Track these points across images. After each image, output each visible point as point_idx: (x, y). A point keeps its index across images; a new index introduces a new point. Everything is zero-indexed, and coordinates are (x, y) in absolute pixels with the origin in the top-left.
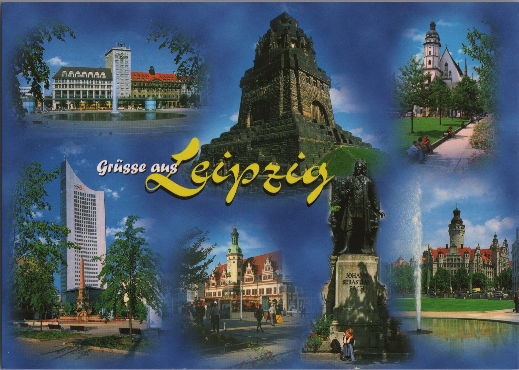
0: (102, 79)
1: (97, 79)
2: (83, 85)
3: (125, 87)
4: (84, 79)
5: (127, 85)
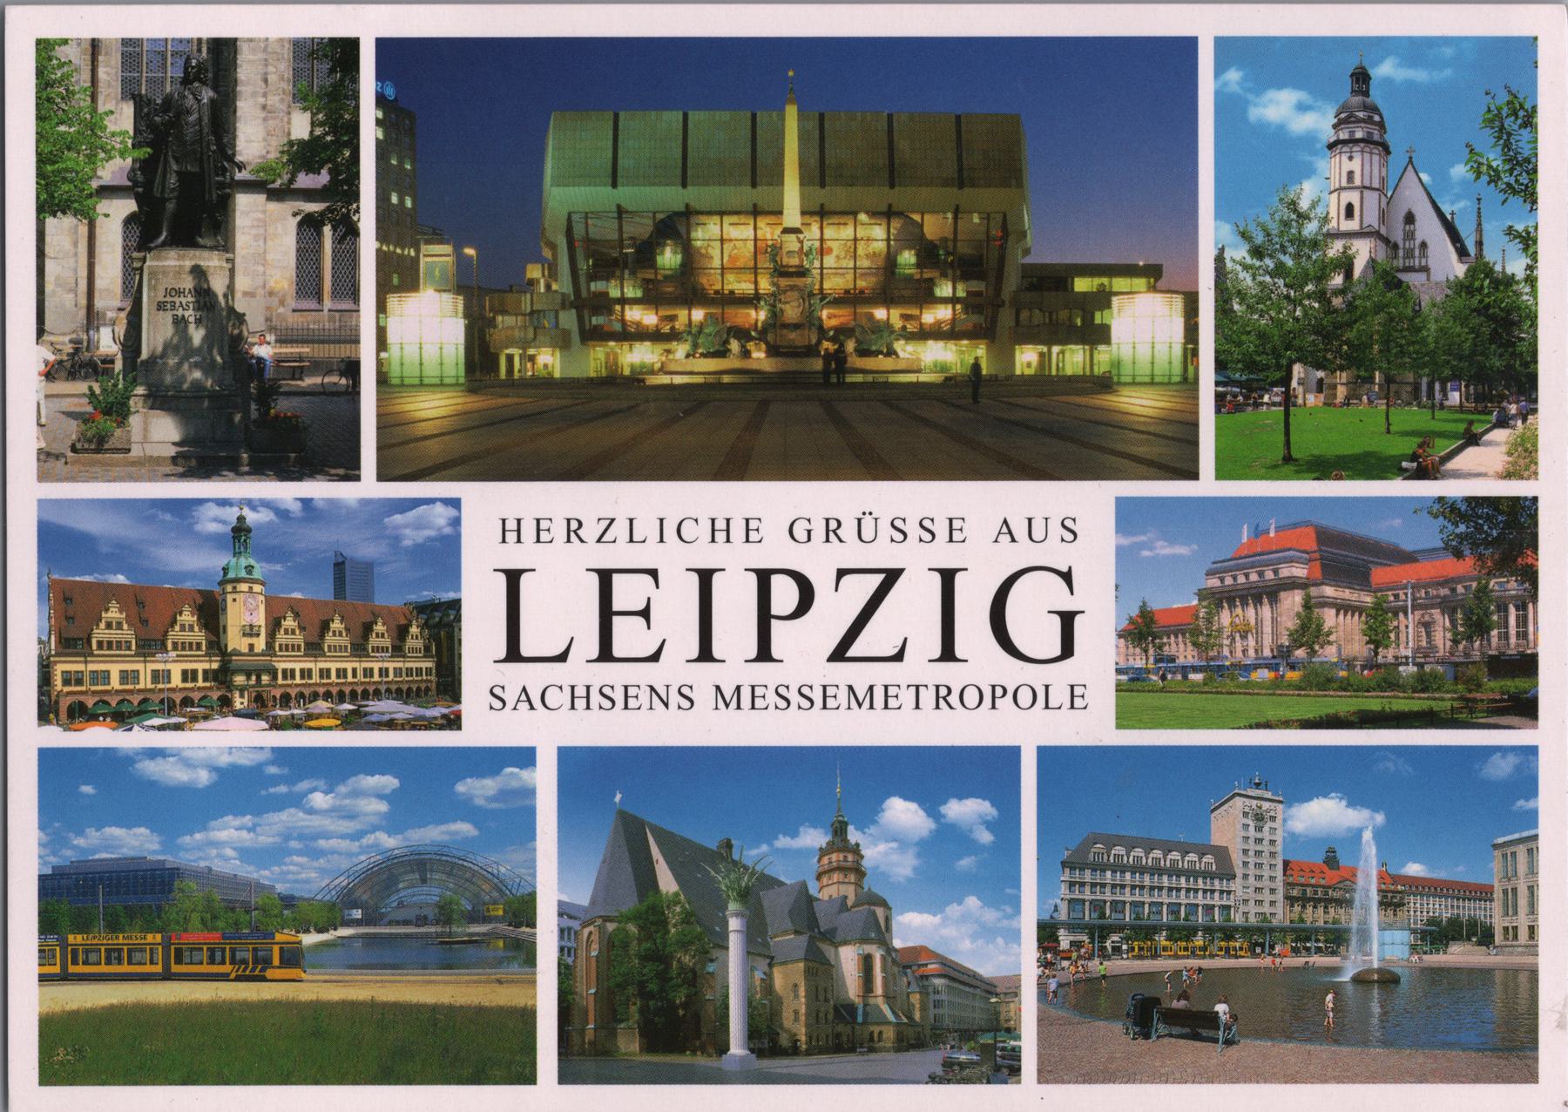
0: (1207, 875)
1: (1191, 873)
2: (1152, 888)
3: (1266, 896)
4: (1157, 870)
5: (1273, 891)
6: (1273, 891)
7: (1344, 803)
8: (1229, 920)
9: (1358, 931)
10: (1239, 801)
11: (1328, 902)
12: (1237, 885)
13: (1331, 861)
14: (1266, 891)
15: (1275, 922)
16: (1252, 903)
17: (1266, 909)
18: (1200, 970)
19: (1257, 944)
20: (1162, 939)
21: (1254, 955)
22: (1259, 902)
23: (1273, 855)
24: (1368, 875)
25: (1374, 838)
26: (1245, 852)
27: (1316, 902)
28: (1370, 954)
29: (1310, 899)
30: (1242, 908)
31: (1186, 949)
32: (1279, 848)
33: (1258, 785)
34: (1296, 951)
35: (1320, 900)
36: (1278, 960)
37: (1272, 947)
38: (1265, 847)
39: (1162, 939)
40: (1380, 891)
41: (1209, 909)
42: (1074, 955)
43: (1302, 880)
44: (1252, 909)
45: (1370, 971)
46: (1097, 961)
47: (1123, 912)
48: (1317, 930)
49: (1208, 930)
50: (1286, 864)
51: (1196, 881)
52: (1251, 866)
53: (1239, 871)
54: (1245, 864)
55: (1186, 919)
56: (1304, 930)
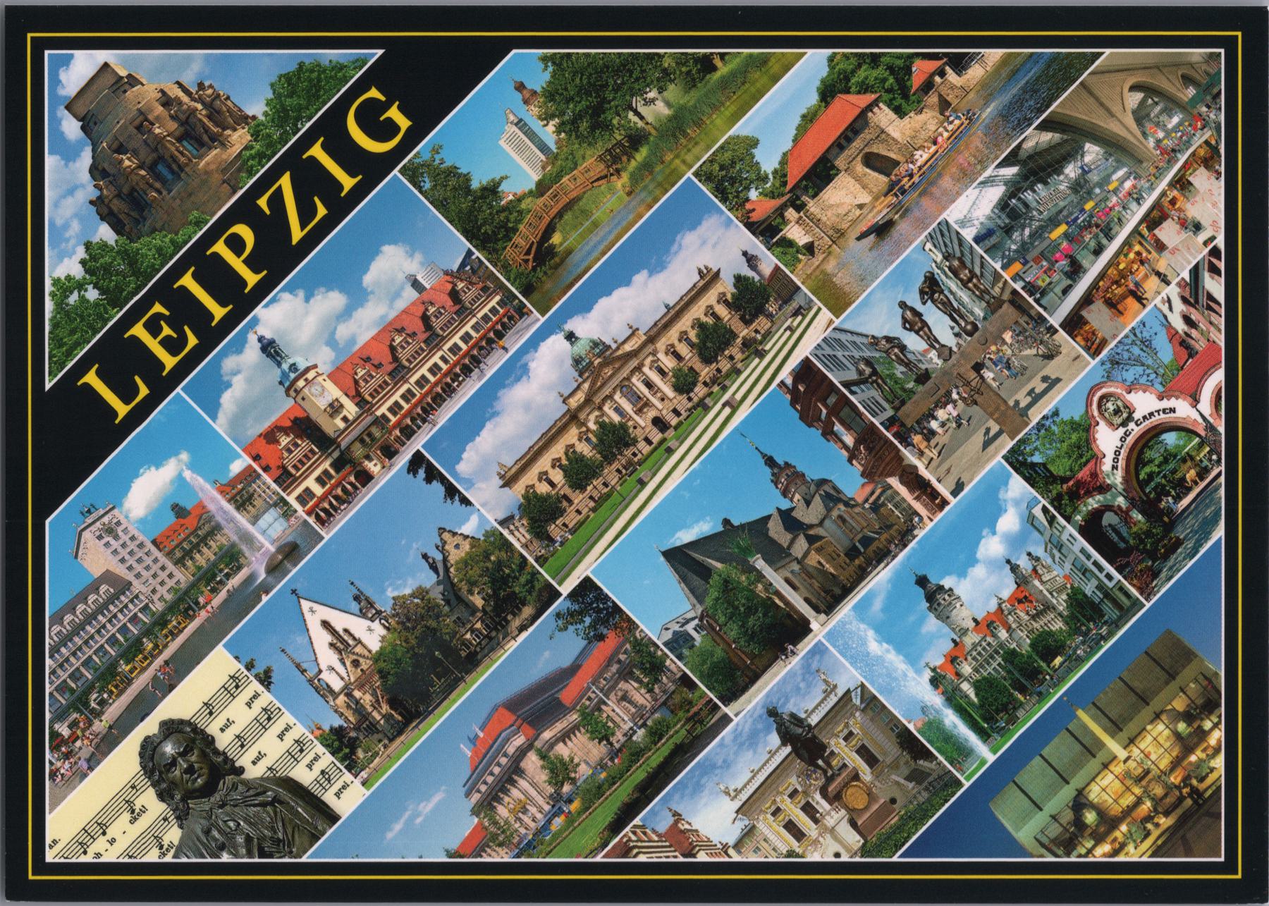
0: (112, 599)
3: (163, 575)
5: (163, 568)
6: (163, 568)
7: (153, 469)
8: (154, 614)
9: (240, 538)
10: (87, 535)
11: (204, 540)
12: (137, 586)
13: (179, 511)
14: (159, 572)
15: (183, 586)
16: (158, 588)
17: (170, 583)
18: (166, 663)
19: (186, 610)
20: (124, 667)
21: (192, 618)
22: (162, 583)
23: (141, 546)
24: (213, 500)
25: (193, 472)
26: (123, 561)
27: (196, 547)
28: (262, 546)
29: (191, 551)
30: (155, 598)
31: (146, 658)
32: (141, 538)
33: (89, 512)
34: (214, 590)
35: (198, 544)
36: (209, 608)
37: (197, 603)
38: (132, 546)
39: (124, 667)
40: (229, 501)
41: (134, 619)
42: (79, 733)
43: (174, 543)
44: (162, 591)
45: (273, 557)
46: (97, 722)
47: (82, 675)
48: (215, 564)
49: (148, 632)
50: (154, 542)
51: (109, 611)
52: (135, 565)
53: (129, 576)
54: (130, 568)
55: (126, 640)
56: (206, 573)
